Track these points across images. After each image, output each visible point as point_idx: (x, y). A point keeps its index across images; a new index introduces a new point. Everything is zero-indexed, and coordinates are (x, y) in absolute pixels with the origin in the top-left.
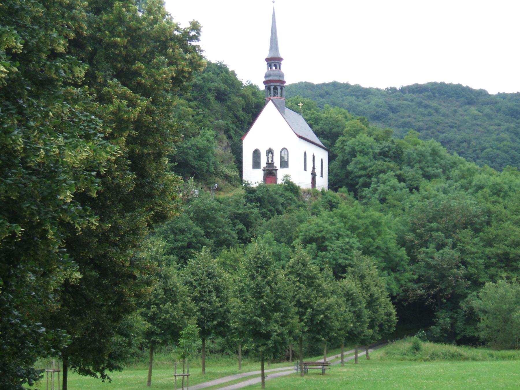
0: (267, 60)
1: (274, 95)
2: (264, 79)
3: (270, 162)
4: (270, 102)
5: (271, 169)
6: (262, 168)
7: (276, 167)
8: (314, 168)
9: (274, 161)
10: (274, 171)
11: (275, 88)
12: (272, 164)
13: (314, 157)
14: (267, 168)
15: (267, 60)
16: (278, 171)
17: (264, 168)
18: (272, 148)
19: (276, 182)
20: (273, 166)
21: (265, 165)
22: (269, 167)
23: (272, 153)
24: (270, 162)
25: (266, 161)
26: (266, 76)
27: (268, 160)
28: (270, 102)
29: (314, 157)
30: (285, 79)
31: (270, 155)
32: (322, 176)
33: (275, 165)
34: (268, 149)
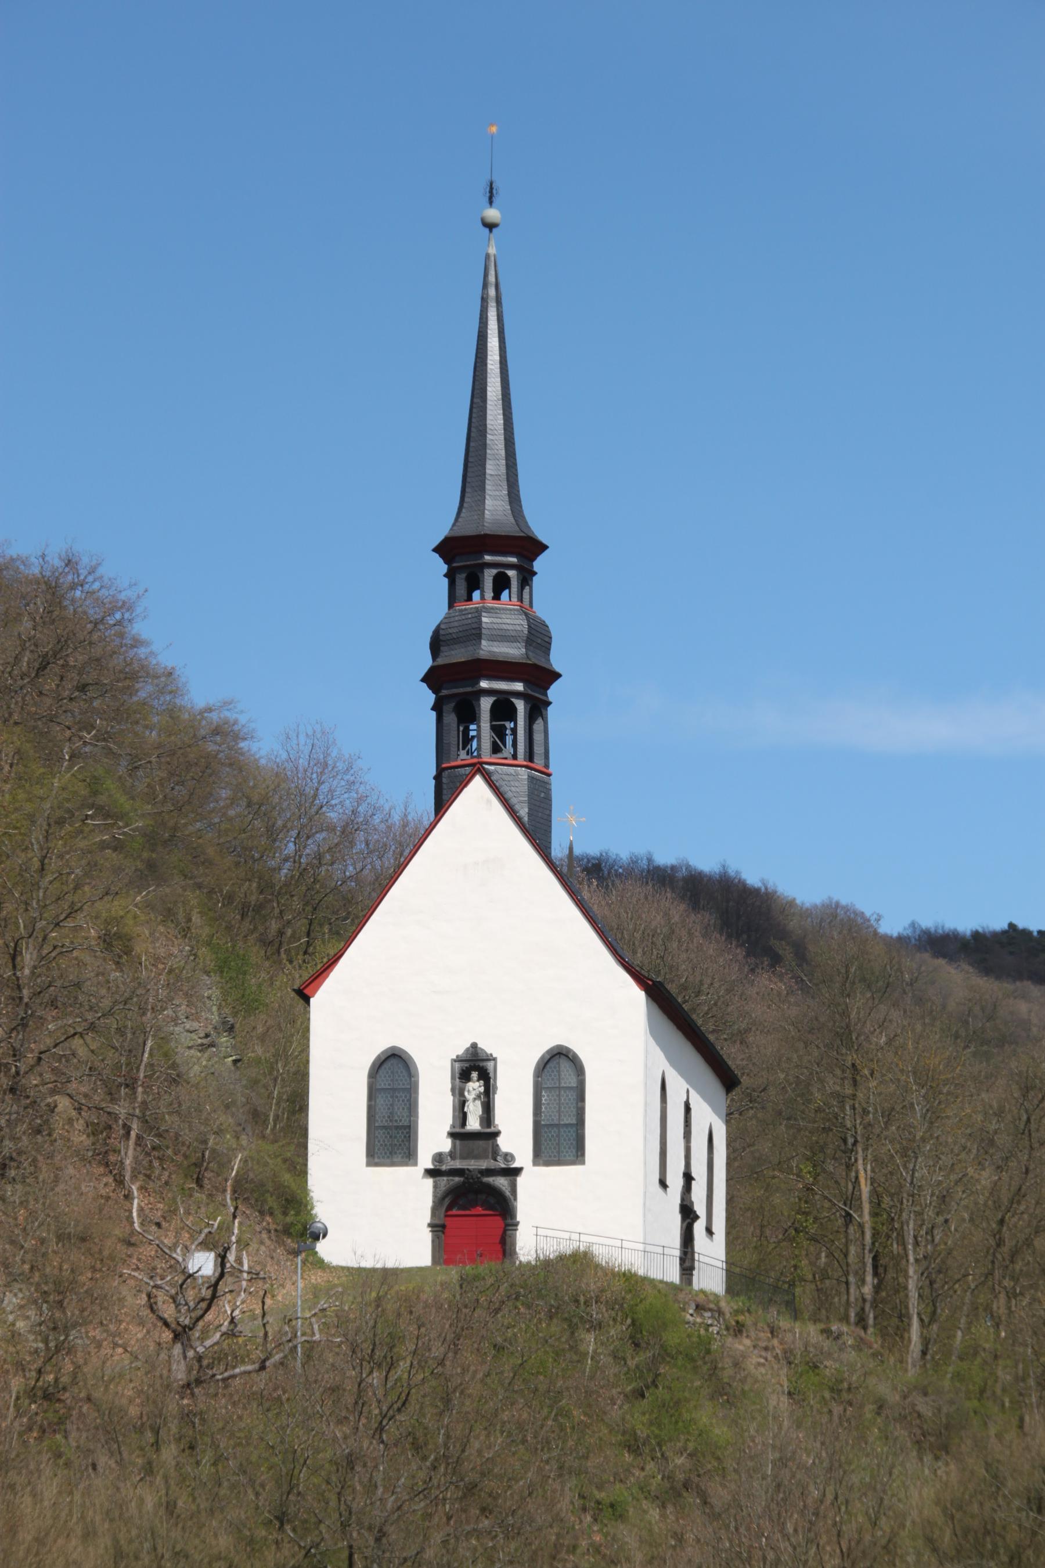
0: (447, 549)
1: (496, 749)
2: (425, 662)
3: (474, 1124)
4: (478, 781)
5: (484, 1164)
6: (425, 1161)
7: (509, 1157)
8: (688, 1178)
9: (500, 1119)
10: (501, 1182)
11: (503, 710)
12: (489, 1135)
13: (688, 1109)
14: (458, 1164)
15: (447, 549)
17: (438, 1158)
18: (487, 1046)
19: (505, 1245)
20: (495, 1151)
21: (446, 1145)
22: (463, 1157)
23: (486, 1078)
24: (474, 1124)
26: (437, 644)
27: (462, 1116)
28: (478, 781)
29: (688, 1109)
30: (557, 661)
31: (475, 1087)
32: (709, 1231)
33: (504, 1143)
34: (460, 1048)
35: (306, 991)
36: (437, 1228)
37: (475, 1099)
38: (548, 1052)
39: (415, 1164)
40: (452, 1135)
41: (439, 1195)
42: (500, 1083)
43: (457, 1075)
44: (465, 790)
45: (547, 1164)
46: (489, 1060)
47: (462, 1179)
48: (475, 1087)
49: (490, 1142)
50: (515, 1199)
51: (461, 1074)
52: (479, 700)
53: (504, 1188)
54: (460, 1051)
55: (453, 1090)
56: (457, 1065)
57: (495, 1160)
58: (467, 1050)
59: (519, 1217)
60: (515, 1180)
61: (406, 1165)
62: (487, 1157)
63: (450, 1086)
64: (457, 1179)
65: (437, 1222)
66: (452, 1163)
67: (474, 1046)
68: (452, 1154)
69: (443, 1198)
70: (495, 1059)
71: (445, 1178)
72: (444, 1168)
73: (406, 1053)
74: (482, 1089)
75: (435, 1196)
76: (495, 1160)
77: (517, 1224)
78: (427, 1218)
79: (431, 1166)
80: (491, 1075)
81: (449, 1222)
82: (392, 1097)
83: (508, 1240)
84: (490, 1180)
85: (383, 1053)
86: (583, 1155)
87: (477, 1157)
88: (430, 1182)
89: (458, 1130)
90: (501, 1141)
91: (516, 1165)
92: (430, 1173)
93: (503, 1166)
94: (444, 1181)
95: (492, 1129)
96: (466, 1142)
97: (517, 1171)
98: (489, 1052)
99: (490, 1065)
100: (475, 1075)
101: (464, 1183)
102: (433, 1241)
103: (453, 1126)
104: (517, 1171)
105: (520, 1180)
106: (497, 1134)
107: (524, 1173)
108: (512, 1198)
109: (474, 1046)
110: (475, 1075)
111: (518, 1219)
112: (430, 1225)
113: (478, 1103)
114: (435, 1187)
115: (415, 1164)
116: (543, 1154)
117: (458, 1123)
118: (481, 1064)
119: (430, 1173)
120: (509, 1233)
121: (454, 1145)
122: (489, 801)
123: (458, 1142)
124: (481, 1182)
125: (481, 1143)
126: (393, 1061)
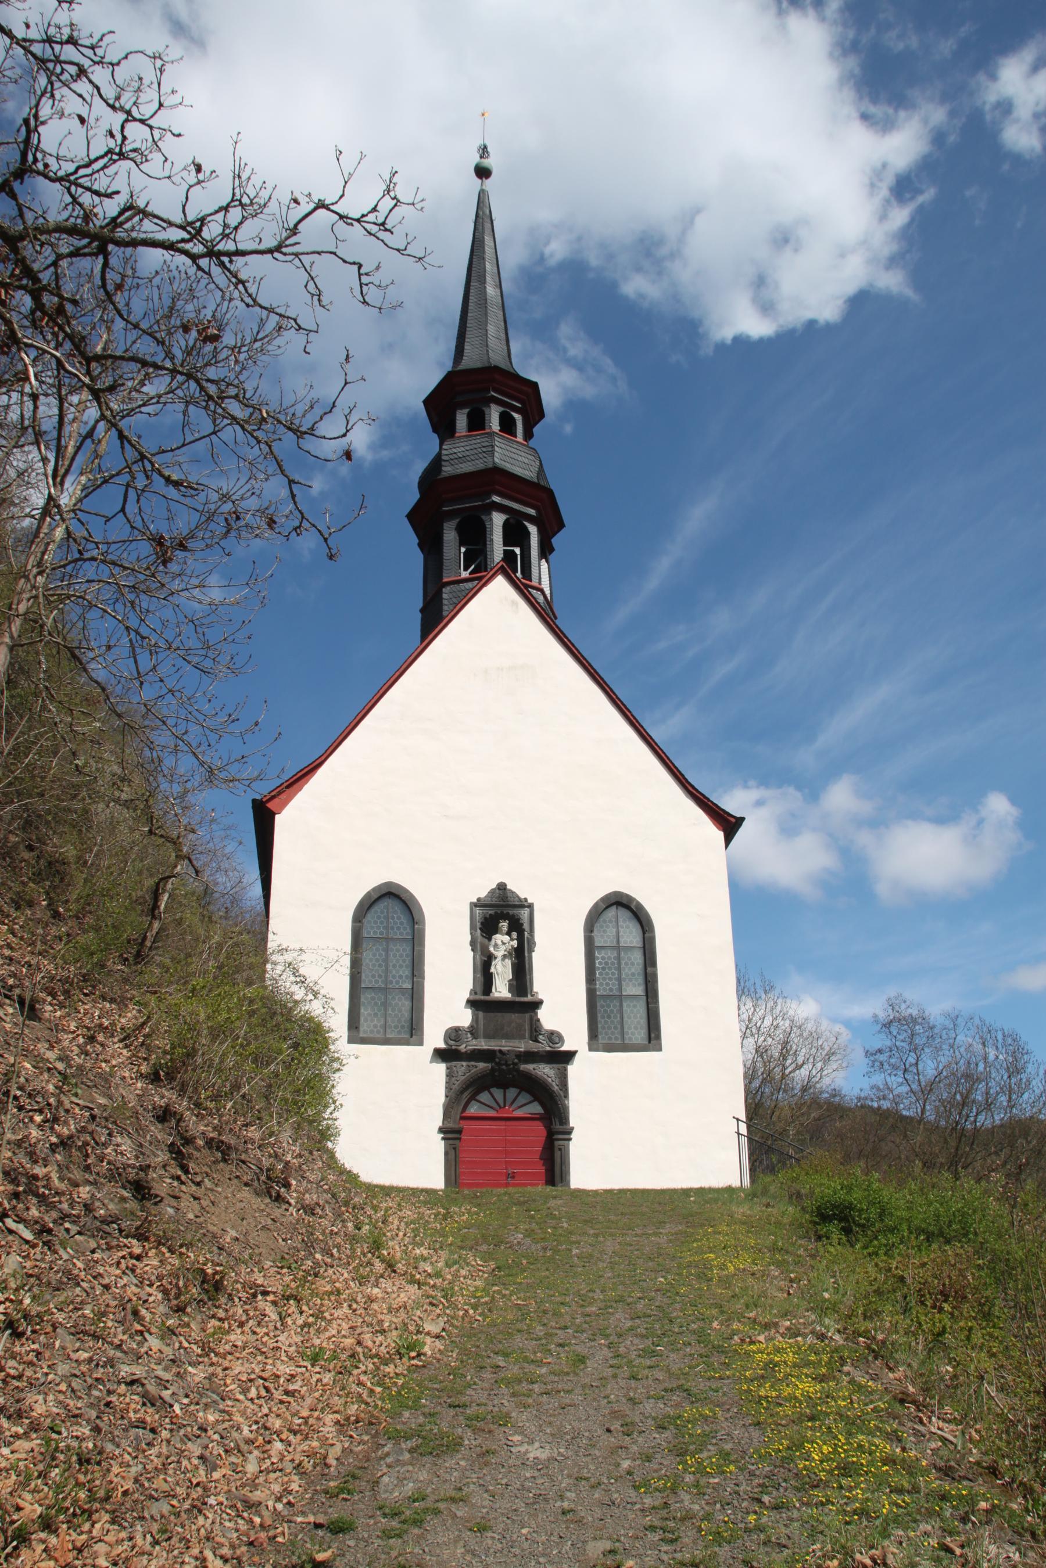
5: (522, 1046)
6: (434, 1037)
7: (554, 1037)
9: (542, 984)
10: (546, 1071)
14: (483, 1044)
16: (574, 1070)
17: (454, 1034)
18: (520, 888)
20: (535, 1029)
21: (465, 1018)
22: (488, 1036)
24: (501, 990)
25: (465, 983)
31: (502, 942)
33: (548, 1018)
34: (482, 890)
35: (270, 805)
36: (450, 1133)
37: (504, 957)
38: (603, 899)
39: (421, 1043)
40: (472, 1003)
41: (456, 1087)
42: (539, 936)
43: (479, 925)
44: (485, 589)
45: (610, 1048)
46: (522, 906)
47: (489, 1065)
48: (502, 942)
49: (527, 1016)
50: (566, 1096)
51: (482, 923)
52: (490, 514)
53: (550, 1080)
54: (483, 893)
55: (473, 943)
56: (478, 911)
57: (537, 1041)
58: (492, 891)
59: (574, 1119)
60: (566, 1070)
61: (407, 1043)
62: (522, 1037)
63: (469, 938)
64: (481, 1065)
65: (450, 1125)
66: (474, 1042)
67: (502, 887)
68: (473, 1030)
69: (462, 1092)
70: (531, 906)
71: (464, 1064)
72: (462, 1048)
73: (406, 891)
74: (515, 943)
75: (449, 1087)
76: (537, 1041)
77: (570, 1131)
78: (439, 1122)
79: (442, 1045)
80: (526, 926)
81: (465, 1125)
82: (387, 950)
83: (557, 1154)
84: (523, 1067)
85: (374, 889)
86: (658, 1037)
87: (508, 1036)
88: (441, 1068)
89: (480, 997)
90: (542, 1014)
91: (565, 1048)
92: (440, 1055)
93: (548, 1049)
94: (462, 1066)
95: (529, 998)
96: (492, 1015)
97: (569, 1056)
98: (522, 896)
99: (524, 913)
100: (504, 925)
101: (493, 1070)
102: (446, 1154)
103: (473, 992)
104: (569, 1056)
105: (572, 1069)
106: (538, 1004)
107: (577, 1058)
108: (562, 1093)
109: (502, 887)
110: (504, 925)
111: (572, 1125)
112: (441, 1130)
113: (508, 962)
114: (450, 1075)
115: (421, 1043)
116: (596, 1039)
117: (479, 990)
118: (511, 912)
119: (440, 1055)
120: (557, 1143)
121: (475, 1018)
122: (514, 603)
123: (481, 1014)
124: (518, 1071)
125: (514, 1017)
126: (387, 902)
